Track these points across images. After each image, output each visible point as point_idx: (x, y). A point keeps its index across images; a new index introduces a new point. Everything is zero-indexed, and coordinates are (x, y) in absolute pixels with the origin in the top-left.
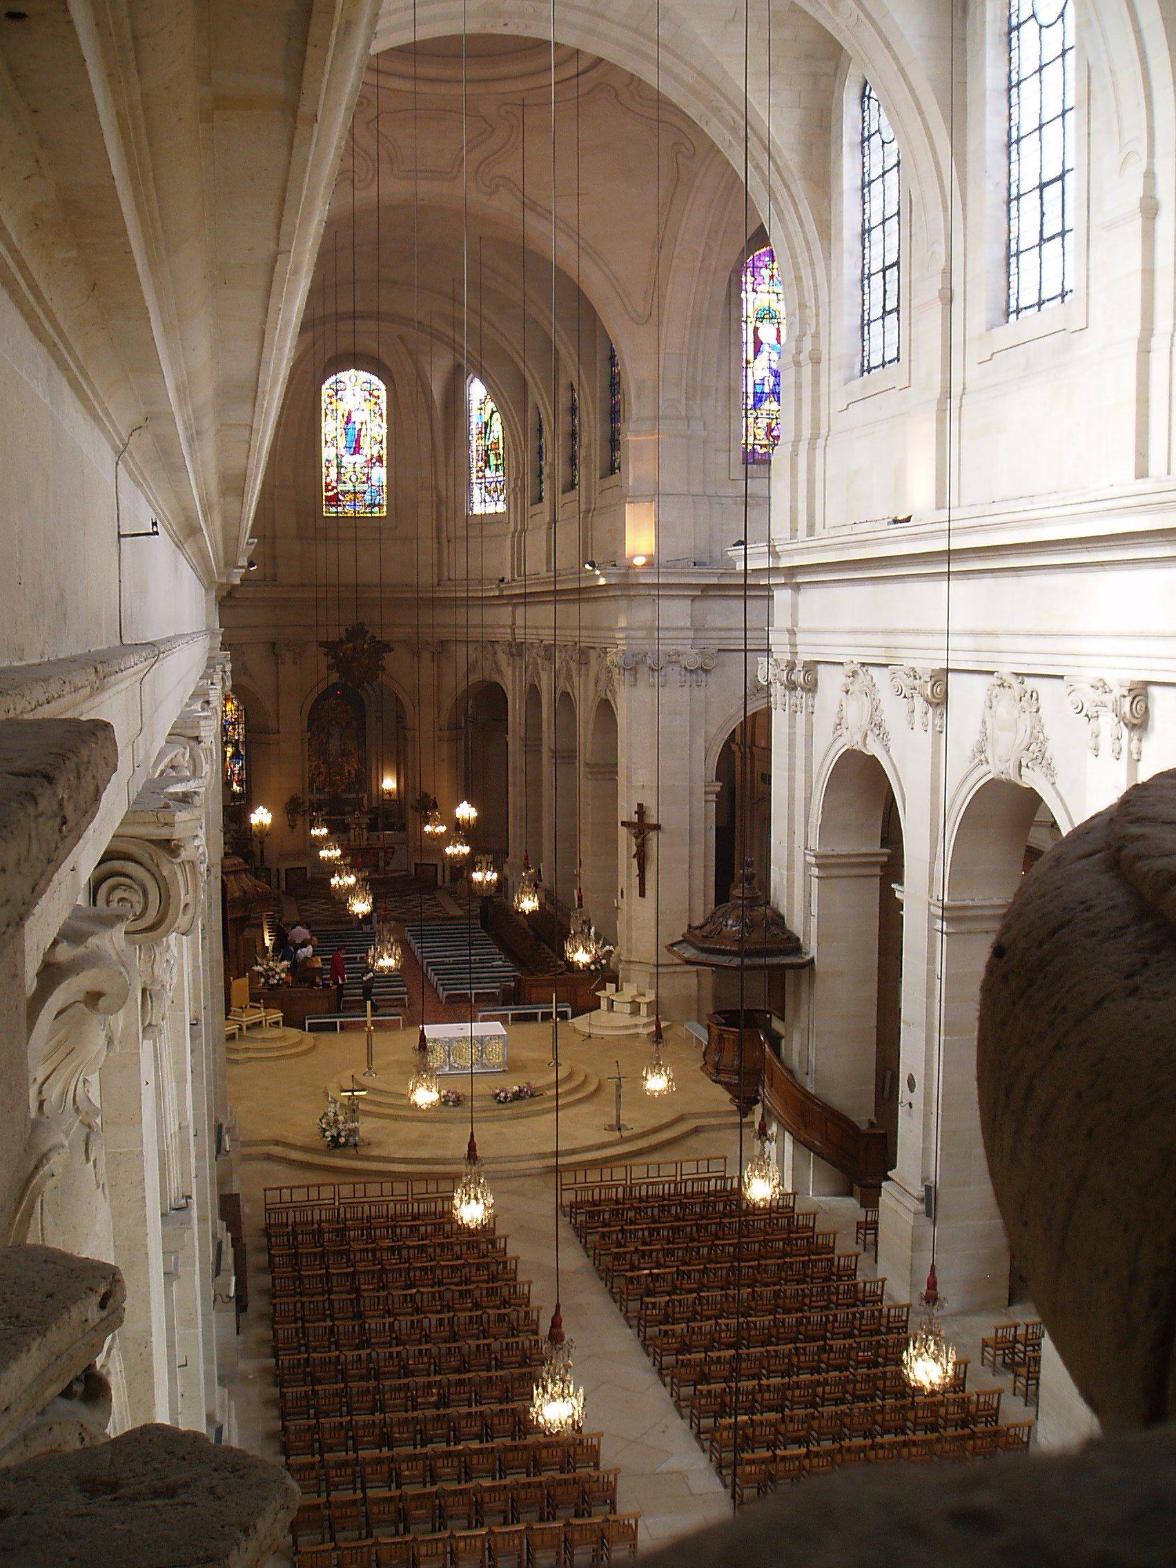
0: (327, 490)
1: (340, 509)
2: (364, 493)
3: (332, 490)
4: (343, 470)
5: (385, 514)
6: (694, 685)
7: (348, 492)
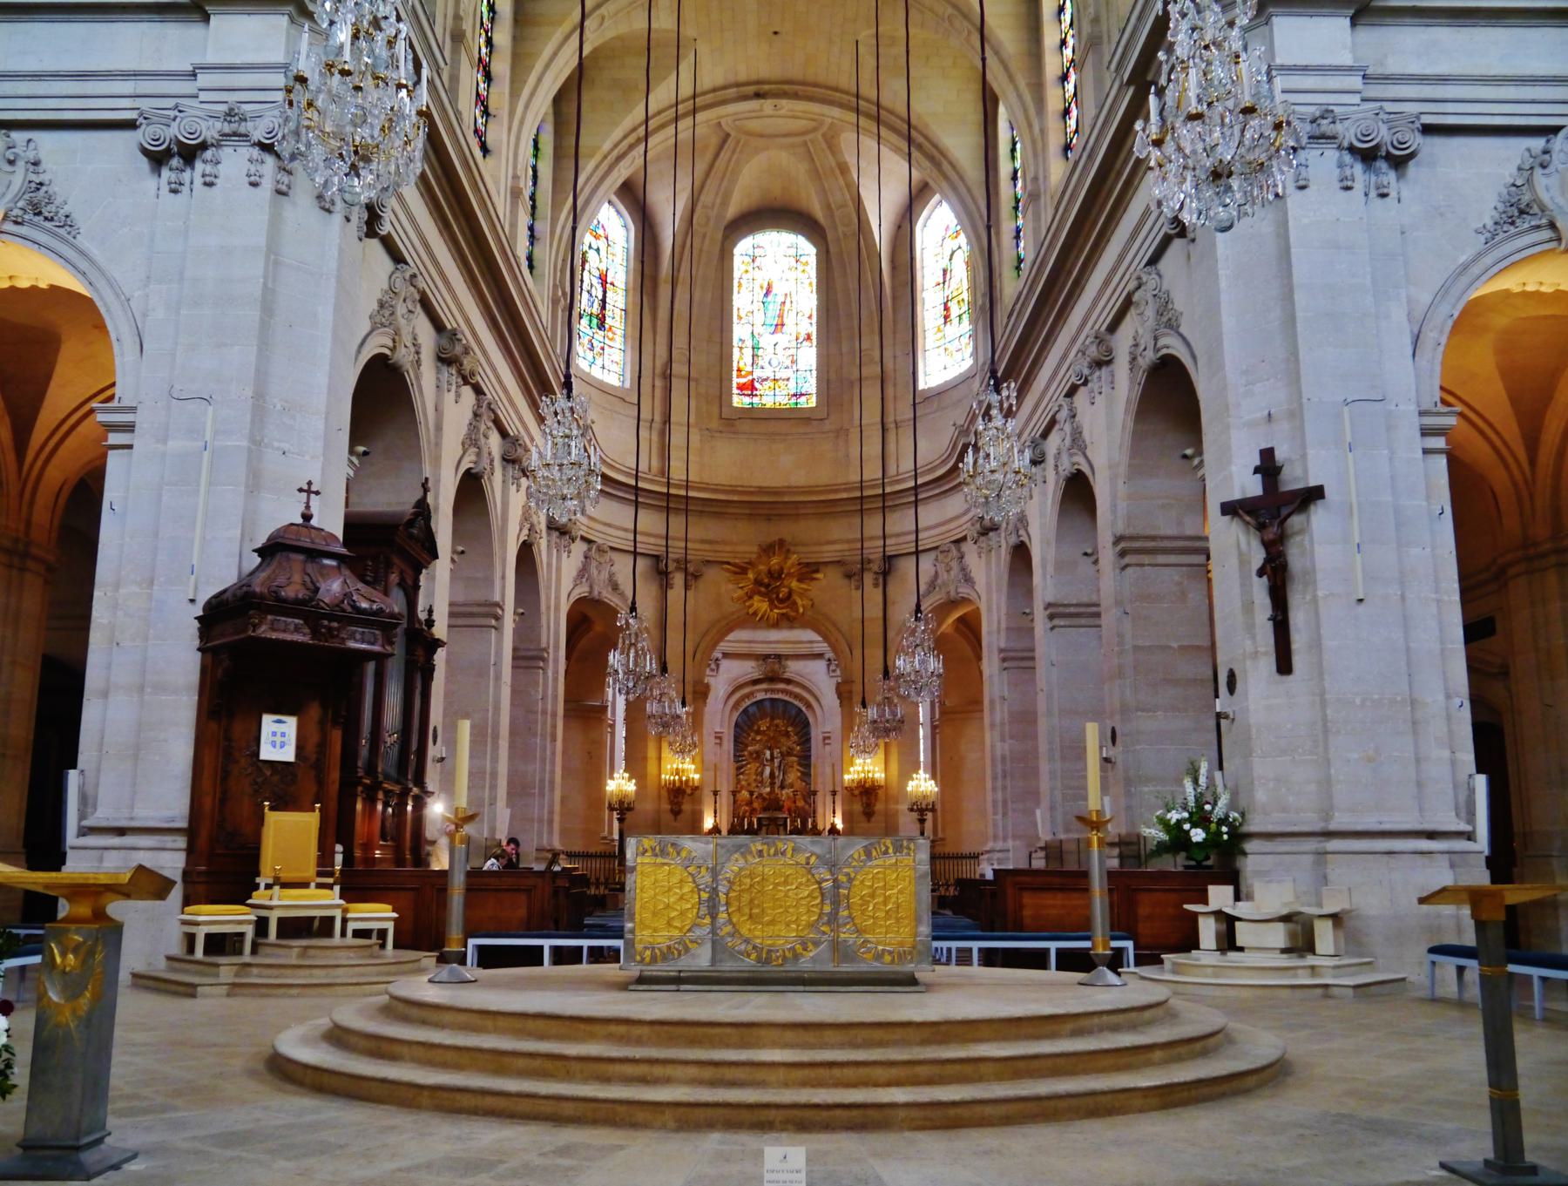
0: (738, 377)
1: (756, 400)
2: (788, 379)
3: (745, 377)
4: (760, 352)
5: (814, 405)
6: (1373, 194)
7: (766, 380)
